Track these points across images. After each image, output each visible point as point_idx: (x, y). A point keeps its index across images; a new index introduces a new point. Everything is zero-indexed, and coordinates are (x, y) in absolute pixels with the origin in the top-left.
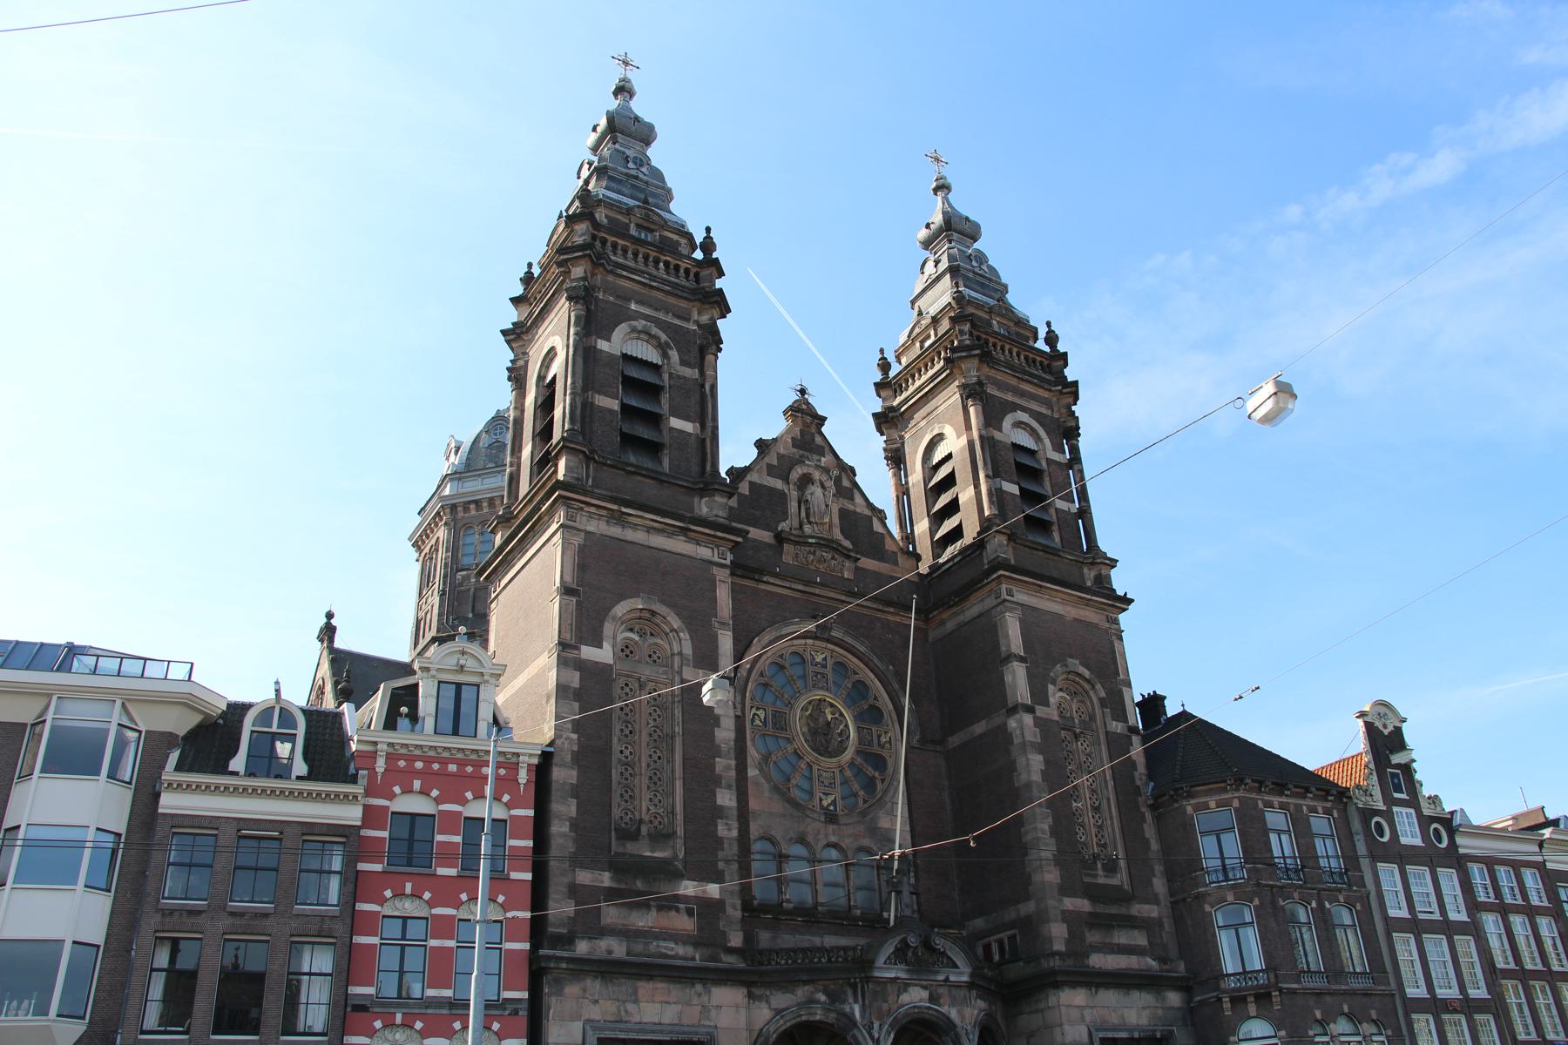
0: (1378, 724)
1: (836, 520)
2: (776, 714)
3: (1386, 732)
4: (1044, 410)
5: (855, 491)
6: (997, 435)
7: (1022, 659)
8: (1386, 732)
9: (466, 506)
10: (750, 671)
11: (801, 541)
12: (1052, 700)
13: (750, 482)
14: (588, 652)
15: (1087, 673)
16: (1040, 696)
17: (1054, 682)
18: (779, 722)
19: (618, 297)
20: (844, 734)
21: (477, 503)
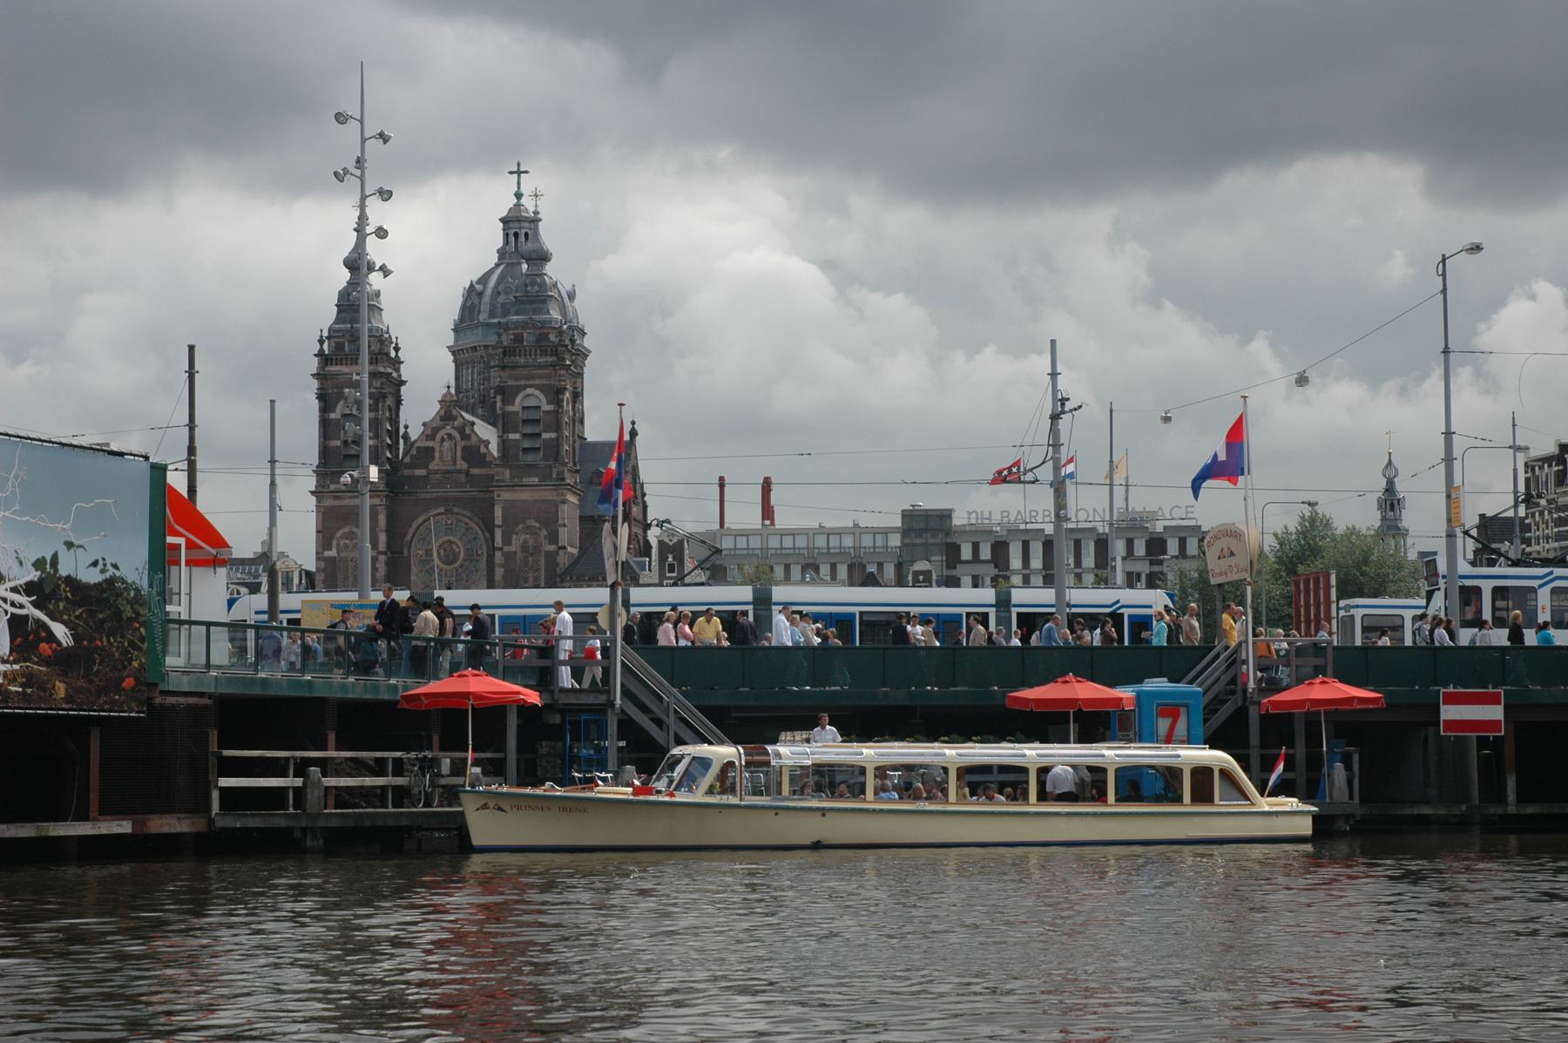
0: (667, 540)
1: (459, 454)
2: (426, 551)
3: (671, 544)
4: (544, 382)
5: (473, 435)
6: (510, 408)
7: (499, 526)
8: (671, 544)
9: (458, 351)
10: (413, 537)
11: (436, 472)
12: (513, 542)
13: (417, 448)
14: (327, 553)
15: (538, 525)
16: (507, 541)
17: (517, 534)
18: (429, 553)
19: (337, 388)
20: (459, 552)
21: (462, 350)
